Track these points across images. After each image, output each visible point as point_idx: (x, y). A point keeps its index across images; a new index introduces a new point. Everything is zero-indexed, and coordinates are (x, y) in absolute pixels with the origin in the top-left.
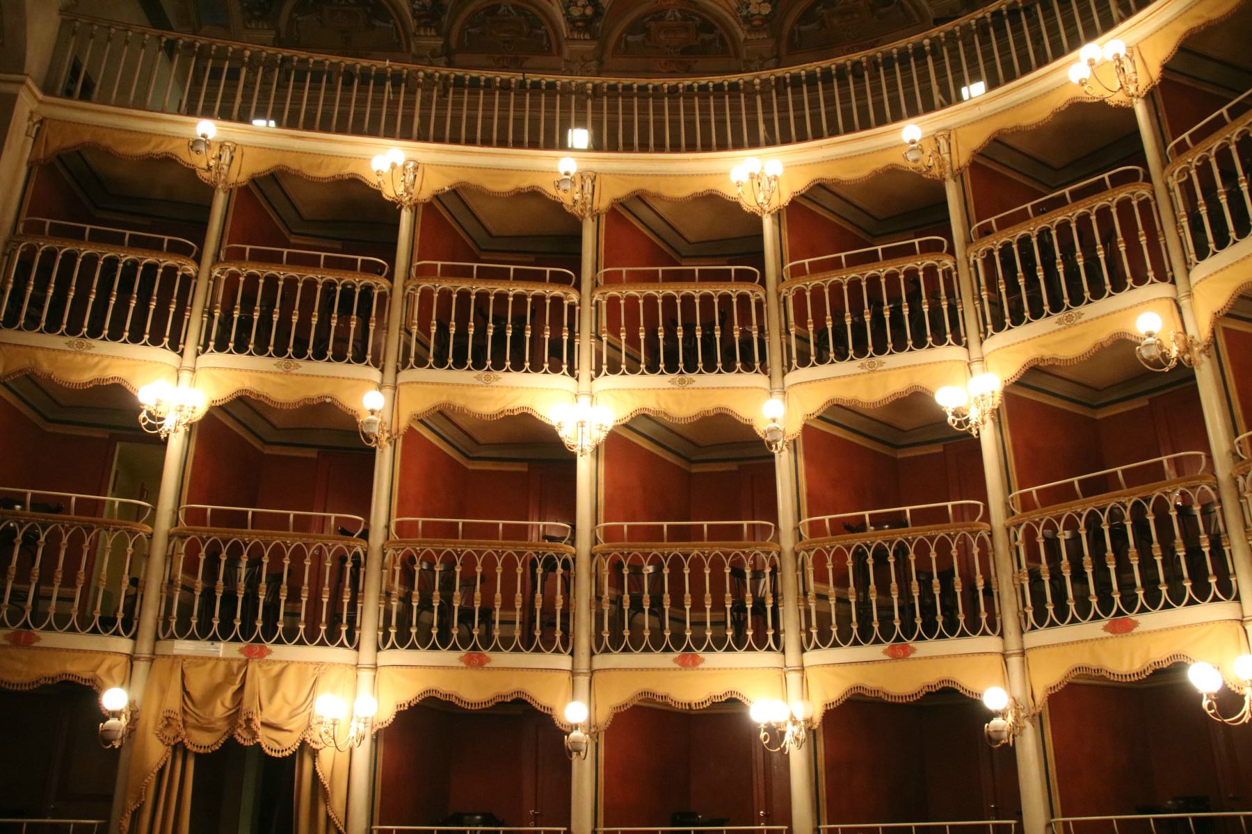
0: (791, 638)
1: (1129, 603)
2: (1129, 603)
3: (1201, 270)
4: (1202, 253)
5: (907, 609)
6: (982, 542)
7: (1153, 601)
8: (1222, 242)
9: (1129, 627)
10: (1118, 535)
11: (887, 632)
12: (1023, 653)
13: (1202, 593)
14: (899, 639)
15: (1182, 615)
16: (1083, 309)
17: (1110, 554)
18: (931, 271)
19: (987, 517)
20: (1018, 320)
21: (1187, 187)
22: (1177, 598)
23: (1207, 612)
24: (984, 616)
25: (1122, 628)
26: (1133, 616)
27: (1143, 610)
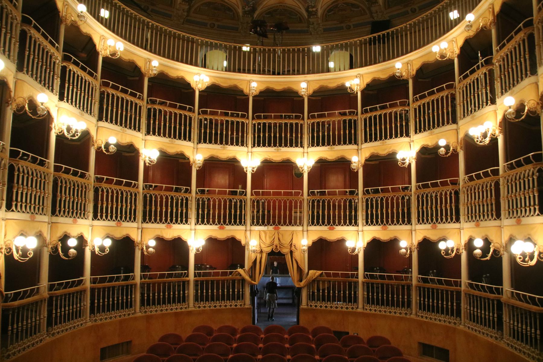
0: (249, 221)
1: (334, 223)
2: (334, 223)
3: (365, 145)
4: (366, 141)
5: (280, 217)
6: (301, 202)
7: (339, 224)
8: (371, 140)
9: (333, 229)
10: (334, 206)
11: (274, 223)
12: (307, 231)
13: (350, 223)
14: (277, 225)
15: (345, 228)
16: (335, 147)
17: (331, 211)
18: (297, 124)
19: (302, 195)
20: (318, 145)
21: (365, 120)
22: (345, 223)
23: (351, 228)
24: (298, 221)
25: (331, 229)
26: (334, 226)
27: (337, 225)
